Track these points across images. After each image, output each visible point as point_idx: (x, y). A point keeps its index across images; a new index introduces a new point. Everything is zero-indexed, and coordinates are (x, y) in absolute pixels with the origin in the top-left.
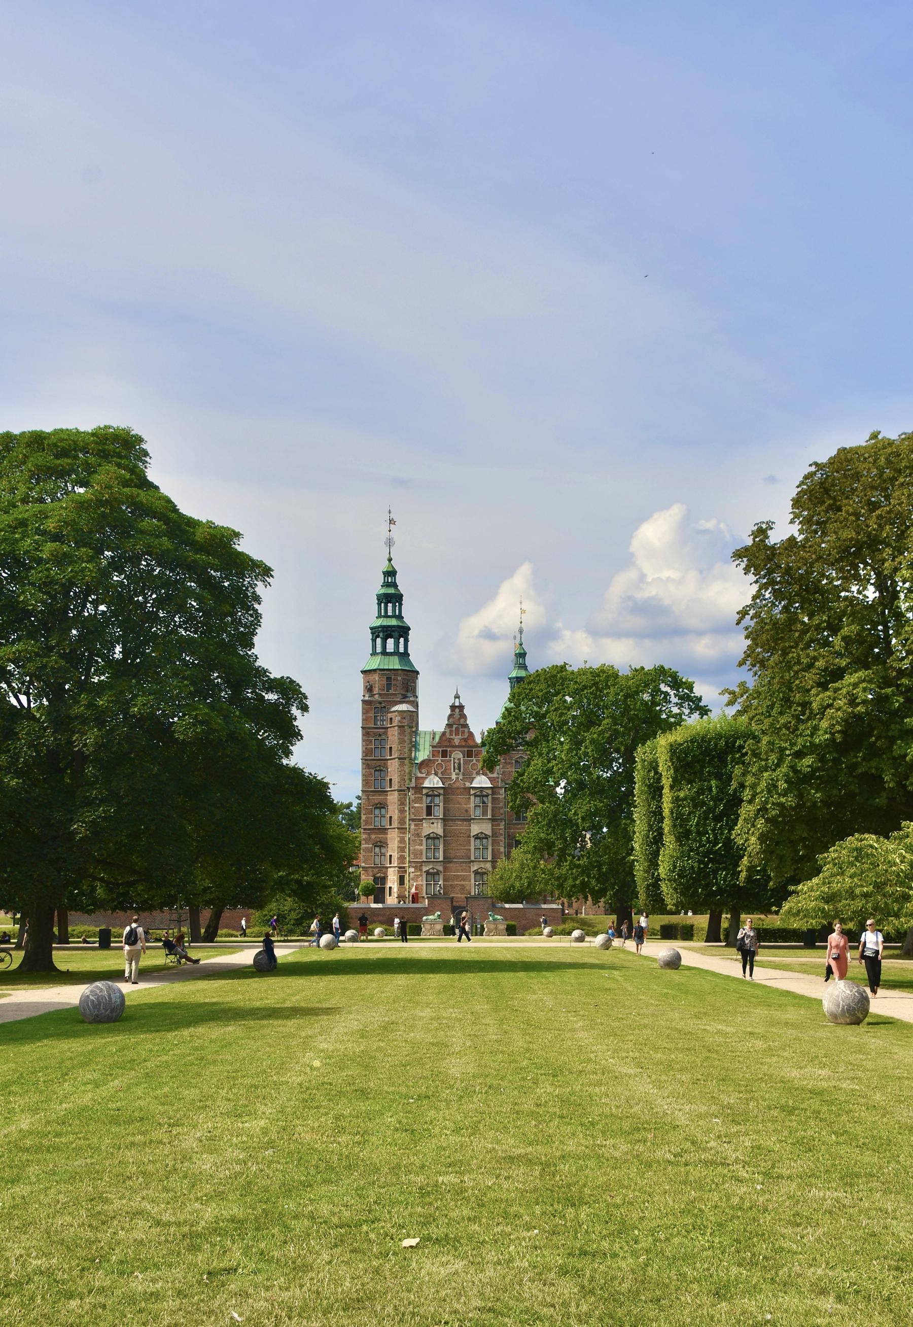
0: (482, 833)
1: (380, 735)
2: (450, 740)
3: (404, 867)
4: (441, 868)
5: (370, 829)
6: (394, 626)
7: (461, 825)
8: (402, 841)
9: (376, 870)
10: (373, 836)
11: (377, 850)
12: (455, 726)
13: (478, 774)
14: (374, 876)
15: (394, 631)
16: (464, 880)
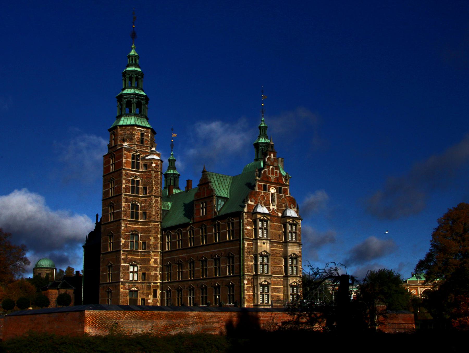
0: (294, 254)
1: (136, 177)
2: (268, 178)
3: (157, 283)
4: (269, 281)
5: (127, 251)
6: (143, 96)
7: (277, 247)
8: (155, 262)
9: (131, 285)
10: (129, 257)
11: (131, 268)
12: (271, 167)
13: (287, 208)
14: (129, 289)
15: (143, 100)
16: (279, 292)
